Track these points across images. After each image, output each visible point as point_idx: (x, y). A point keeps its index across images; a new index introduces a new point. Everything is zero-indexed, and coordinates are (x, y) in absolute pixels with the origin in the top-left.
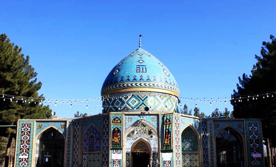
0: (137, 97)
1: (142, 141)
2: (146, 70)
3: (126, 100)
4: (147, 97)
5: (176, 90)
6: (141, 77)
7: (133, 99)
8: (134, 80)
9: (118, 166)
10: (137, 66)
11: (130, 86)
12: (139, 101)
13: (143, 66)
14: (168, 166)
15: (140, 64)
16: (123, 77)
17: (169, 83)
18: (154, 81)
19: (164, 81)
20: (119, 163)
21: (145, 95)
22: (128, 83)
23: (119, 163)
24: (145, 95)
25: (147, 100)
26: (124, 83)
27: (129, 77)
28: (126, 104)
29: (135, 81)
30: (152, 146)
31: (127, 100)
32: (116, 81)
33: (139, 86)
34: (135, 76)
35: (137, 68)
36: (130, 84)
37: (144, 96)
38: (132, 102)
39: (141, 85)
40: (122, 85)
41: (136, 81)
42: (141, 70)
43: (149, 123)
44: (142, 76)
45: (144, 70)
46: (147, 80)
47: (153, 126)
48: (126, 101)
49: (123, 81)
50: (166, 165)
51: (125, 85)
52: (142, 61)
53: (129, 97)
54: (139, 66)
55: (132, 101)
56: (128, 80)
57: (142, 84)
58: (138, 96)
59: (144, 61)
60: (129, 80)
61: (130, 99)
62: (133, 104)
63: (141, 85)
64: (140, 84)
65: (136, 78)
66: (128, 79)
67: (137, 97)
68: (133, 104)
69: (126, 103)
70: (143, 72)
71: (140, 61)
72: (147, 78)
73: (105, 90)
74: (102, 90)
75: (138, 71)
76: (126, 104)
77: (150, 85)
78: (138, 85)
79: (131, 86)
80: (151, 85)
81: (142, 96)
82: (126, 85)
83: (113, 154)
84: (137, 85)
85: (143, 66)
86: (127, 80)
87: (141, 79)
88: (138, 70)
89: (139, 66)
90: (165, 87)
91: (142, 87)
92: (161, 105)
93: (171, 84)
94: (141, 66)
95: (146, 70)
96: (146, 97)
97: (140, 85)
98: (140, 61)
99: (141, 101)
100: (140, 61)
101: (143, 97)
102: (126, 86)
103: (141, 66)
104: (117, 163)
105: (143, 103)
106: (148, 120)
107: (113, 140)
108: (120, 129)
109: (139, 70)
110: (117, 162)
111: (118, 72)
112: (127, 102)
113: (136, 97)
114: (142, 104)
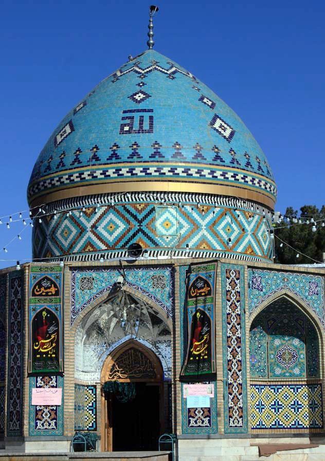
0: (121, 209)
1: (136, 347)
2: (151, 124)
3: (89, 221)
4: (153, 210)
5: (256, 182)
6: (135, 147)
7: (111, 216)
8: (110, 158)
9: (50, 424)
10: (125, 112)
11: (101, 179)
12: (128, 222)
13: (144, 111)
14: (47, 427)
15: (134, 106)
16: (79, 150)
17: (228, 161)
19: (210, 155)
20: (53, 416)
21: (147, 205)
22: (94, 167)
23: (53, 416)
24: (147, 205)
25: (153, 220)
26: (52, 175)
27: (97, 149)
28: (89, 234)
29: (114, 160)
30: (167, 363)
31: (93, 221)
32: (62, 162)
33: (129, 177)
34: (115, 145)
35: (123, 119)
36: (101, 172)
37: (142, 206)
38: (108, 228)
39: (133, 174)
40: (77, 175)
42: (136, 126)
43: (144, 291)
44: (136, 144)
45: (146, 126)
46: (153, 156)
48: (89, 225)
49: (80, 162)
50: (196, 422)
53: (99, 213)
54: (131, 111)
55: (108, 223)
56: (96, 158)
57: (137, 171)
58: (125, 209)
60: (97, 159)
61: (100, 218)
62: (111, 234)
63: (133, 174)
64: (131, 171)
65: (118, 153)
66: (95, 155)
67: (121, 209)
68: (111, 234)
69: (89, 229)
70: (141, 130)
71: (137, 97)
72: (153, 151)
73: (39, 190)
74: (29, 189)
75: (127, 128)
76: (89, 234)
77: (162, 171)
79: (103, 176)
80: (165, 170)
81: (137, 209)
82: (89, 175)
83: (34, 390)
84: (121, 172)
85: (144, 111)
86: (93, 158)
87: (132, 156)
88: (125, 125)
89: (131, 111)
90: (211, 176)
91: (135, 179)
92: (201, 233)
93: (235, 165)
94: (139, 111)
95: (151, 124)
96: (149, 208)
97: (129, 174)
98: (135, 94)
101: (140, 212)
102: (88, 178)
103: (139, 111)
104: (46, 418)
105: (140, 230)
106: (142, 284)
107: (36, 346)
108: (57, 314)
109: (128, 125)
110: (46, 415)
112: (94, 226)
113: (118, 212)
114: (137, 232)
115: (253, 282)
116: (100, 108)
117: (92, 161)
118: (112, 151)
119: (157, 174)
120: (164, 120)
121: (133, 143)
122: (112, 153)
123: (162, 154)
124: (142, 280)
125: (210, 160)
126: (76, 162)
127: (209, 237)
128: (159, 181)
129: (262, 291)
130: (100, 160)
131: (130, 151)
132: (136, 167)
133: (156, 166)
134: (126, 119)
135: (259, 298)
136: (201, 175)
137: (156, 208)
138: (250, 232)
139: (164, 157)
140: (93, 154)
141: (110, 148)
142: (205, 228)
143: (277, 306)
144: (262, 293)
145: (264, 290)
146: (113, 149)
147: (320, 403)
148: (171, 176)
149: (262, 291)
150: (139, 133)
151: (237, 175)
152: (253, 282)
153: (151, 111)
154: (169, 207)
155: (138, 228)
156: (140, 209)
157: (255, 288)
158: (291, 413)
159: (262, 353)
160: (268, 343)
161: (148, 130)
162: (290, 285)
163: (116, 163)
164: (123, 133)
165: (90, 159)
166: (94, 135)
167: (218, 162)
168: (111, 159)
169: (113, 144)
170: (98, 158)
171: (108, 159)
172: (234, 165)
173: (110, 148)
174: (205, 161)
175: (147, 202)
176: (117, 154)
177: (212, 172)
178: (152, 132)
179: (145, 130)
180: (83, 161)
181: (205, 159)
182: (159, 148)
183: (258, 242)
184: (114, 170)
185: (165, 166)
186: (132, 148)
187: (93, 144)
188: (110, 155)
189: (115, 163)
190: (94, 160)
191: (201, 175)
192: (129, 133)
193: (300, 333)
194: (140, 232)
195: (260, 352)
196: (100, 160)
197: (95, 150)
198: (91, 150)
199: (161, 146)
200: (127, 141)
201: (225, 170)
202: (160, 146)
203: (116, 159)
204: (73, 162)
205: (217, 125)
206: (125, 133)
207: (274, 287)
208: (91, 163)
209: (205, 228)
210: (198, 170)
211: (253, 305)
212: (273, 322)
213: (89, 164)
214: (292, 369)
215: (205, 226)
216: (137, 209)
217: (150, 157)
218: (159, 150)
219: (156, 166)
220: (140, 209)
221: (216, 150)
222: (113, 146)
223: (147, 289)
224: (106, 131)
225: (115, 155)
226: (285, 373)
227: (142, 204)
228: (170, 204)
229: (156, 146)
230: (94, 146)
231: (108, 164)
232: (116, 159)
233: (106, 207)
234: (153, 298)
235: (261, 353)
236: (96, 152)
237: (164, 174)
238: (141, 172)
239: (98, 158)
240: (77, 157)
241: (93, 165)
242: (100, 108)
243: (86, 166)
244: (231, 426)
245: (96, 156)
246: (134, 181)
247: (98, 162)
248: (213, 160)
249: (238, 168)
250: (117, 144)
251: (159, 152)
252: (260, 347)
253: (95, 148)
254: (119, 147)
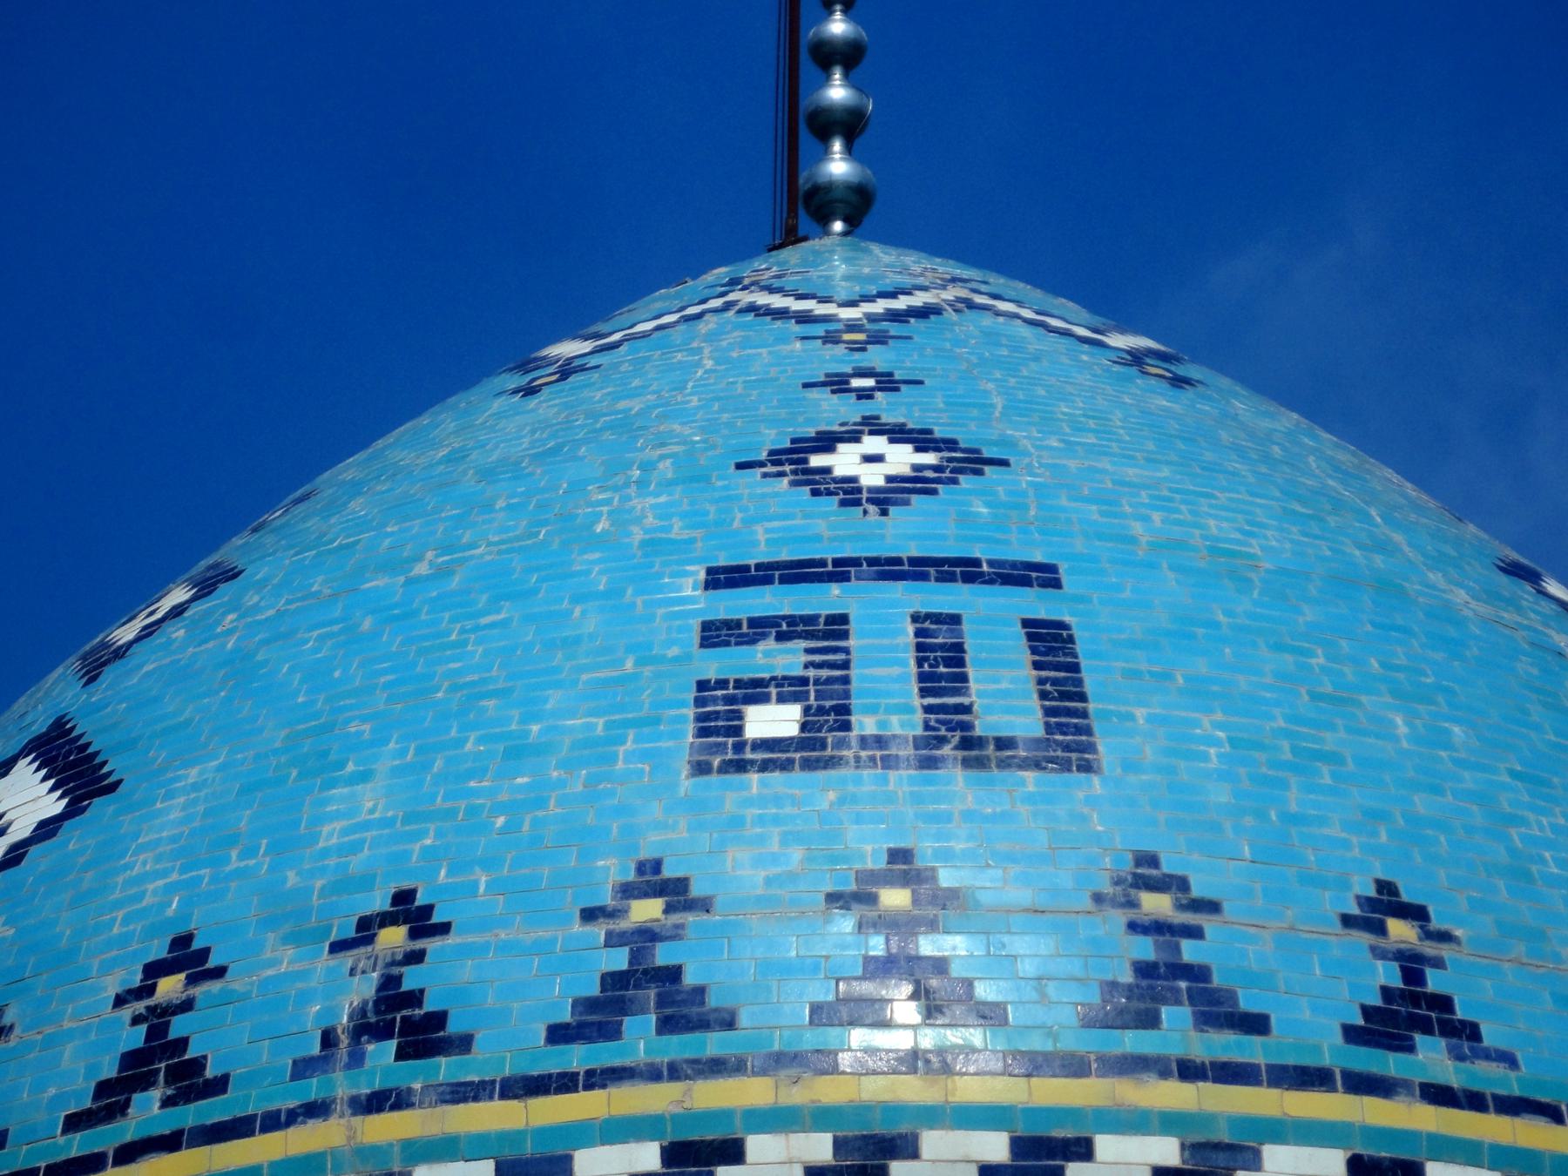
10: (722, 578)
13: (965, 570)
18: (1389, 1064)
35: (715, 634)
41: (679, 1046)
52: (922, 440)
54: (799, 572)
59: (975, 462)
71: (844, 461)
85: (965, 570)
86: (368, 1028)
88: (755, 691)
89: (799, 572)
94: (889, 569)
98: (827, 442)
100: (844, 461)
103: (889, 569)
109: (791, 688)
111: (47, 829)
116: (422, 569)
117: (357, 1059)
118: (613, 940)
120: (1201, 666)
121: (872, 855)
122: (619, 960)
123: (1231, 996)
126: (146, 1082)
130: (464, 1044)
133: (1167, 1123)
134: (752, 640)
139: (1256, 1024)
140: (365, 988)
141: (589, 915)
146: (623, 925)
150: (929, 763)
153: (1045, 576)
161: (1036, 743)
163: (675, 1072)
164: (740, 766)
165: (328, 1040)
166: (370, 800)
168: (610, 1032)
170: (439, 1019)
171: (558, 1034)
173: (589, 915)
176: (673, 974)
178: (1086, 767)
179: (1003, 743)
180: (237, 1072)
182: (1195, 933)
186: (858, 910)
187: (366, 882)
188: (594, 990)
189: (653, 1074)
190: (382, 1053)
192: (808, 765)
196: (464, 1044)
197: (393, 938)
198: (338, 947)
199: (1212, 907)
200: (785, 840)
202: (1199, 906)
203: (667, 1025)
204: (103, 1089)
206: (765, 766)
208: (342, 1084)
213: (313, 1089)
218: (1190, 951)
219: (1167, 1123)
222: (628, 891)
224: (518, 752)
229: (1157, 904)
230: (379, 902)
231: (566, 1083)
232: (667, 1025)
236: (416, 957)
239: (439, 1019)
240: (157, 1031)
241: (376, 1103)
242: (422, 569)
243: (274, 1122)
245: (415, 998)
247: (445, 1068)
250: (668, 872)
251: (1197, 974)
253: (386, 919)
254: (704, 905)
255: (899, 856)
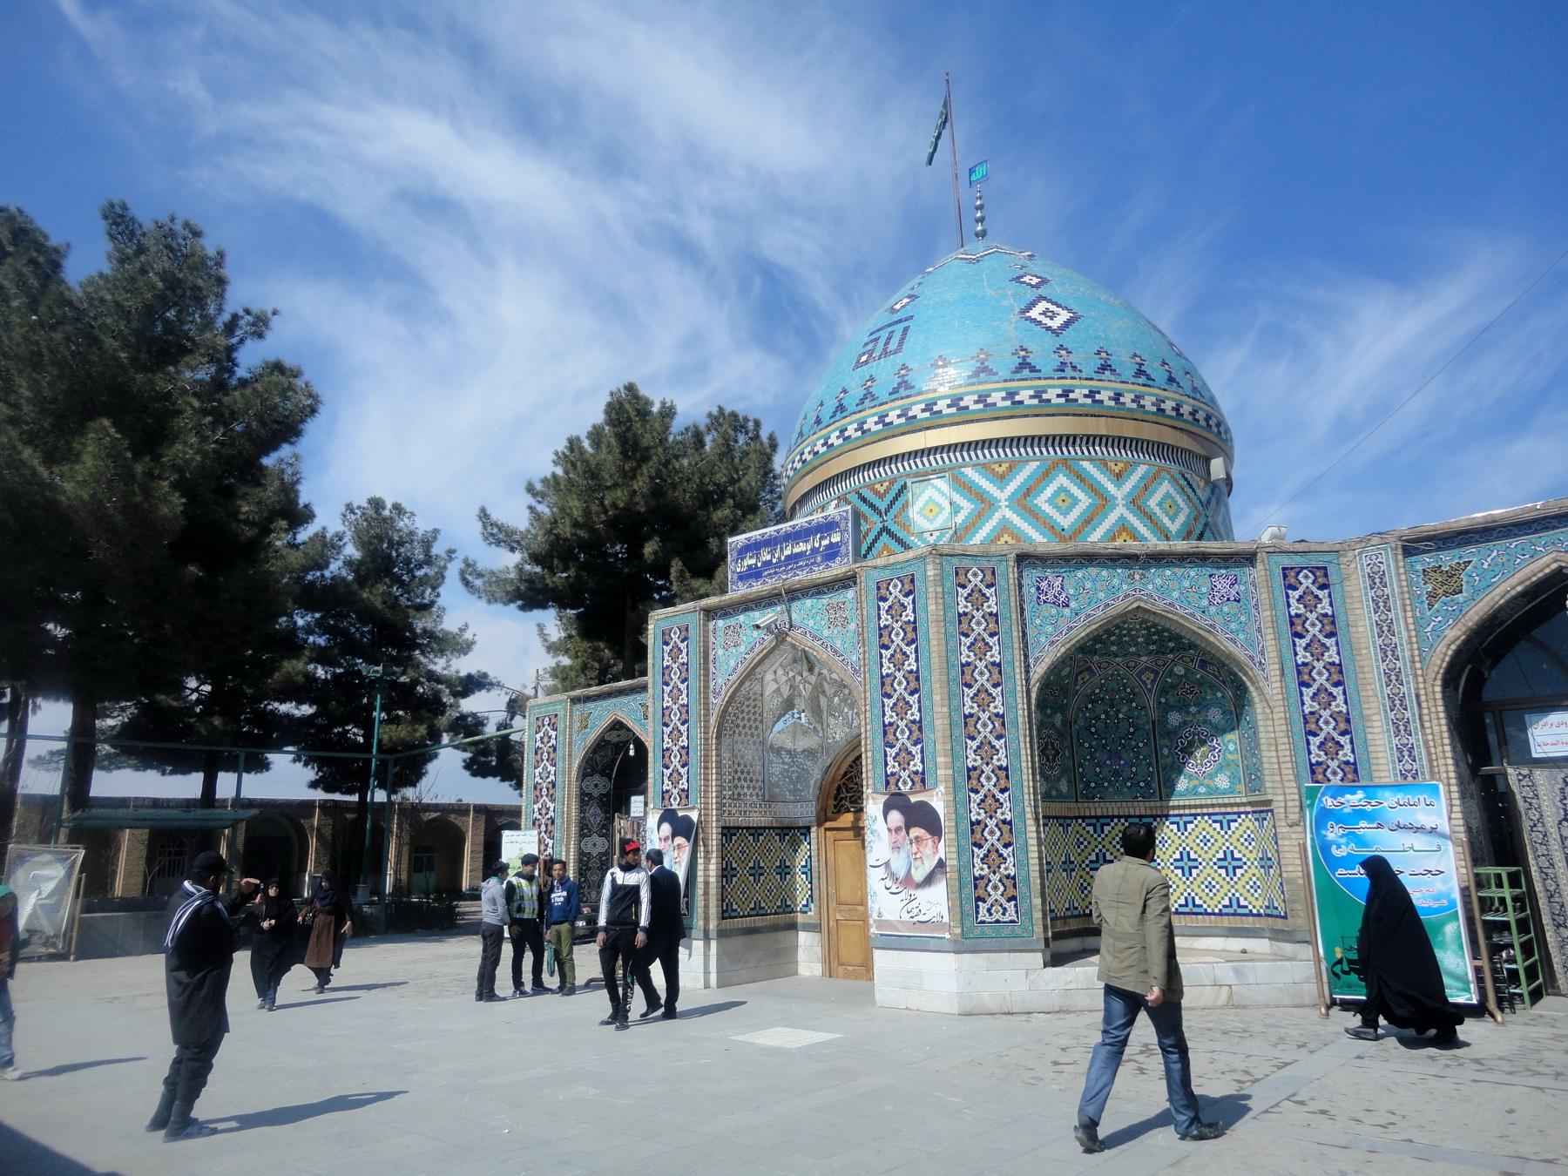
4: (904, 487)
5: (1127, 399)
21: (893, 481)
24: (893, 481)
25: (905, 506)
43: (815, 637)
44: (872, 379)
47: (836, 652)
51: (806, 451)
57: (871, 424)
78: (849, 437)
80: (916, 410)
81: (876, 492)
92: (998, 516)
96: (896, 487)
99: (876, 518)
101: (881, 496)
105: (885, 530)
106: (811, 623)
115: (1038, 588)
119: (903, 420)
124: (811, 615)
125: (1004, 373)
127: (1017, 520)
128: (908, 432)
129: (1067, 606)
131: (862, 392)
132: (868, 417)
135: (1059, 622)
136: (986, 405)
137: (909, 484)
138: (1123, 499)
142: (1007, 503)
143: (1140, 640)
144: (1066, 611)
145: (1073, 604)
147: (1276, 855)
148: (926, 419)
149: (1067, 606)
151: (1073, 392)
152: (1038, 588)
154: (931, 477)
155: (881, 526)
156: (882, 491)
157: (1045, 602)
158: (1220, 879)
159: (1141, 745)
160: (1154, 722)
162: (1150, 587)
167: (1026, 373)
169: (840, 390)
172: (1063, 375)
174: (996, 378)
175: (892, 476)
177: (1011, 395)
181: (996, 374)
183: (1150, 518)
184: (837, 433)
185: (914, 404)
191: (986, 405)
193: (1219, 695)
194: (884, 534)
195: (1133, 743)
201: (1041, 386)
205: (1034, 313)
207: (1101, 595)
209: (1007, 503)
210: (980, 396)
211: (1043, 639)
212: (1152, 676)
214: (1212, 776)
215: (1006, 500)
216: (876, 492)
217: (890, 394)
218: (906, 378)
220: (882, 491)
221: (1023, 353)
223: (819, 632)
225: (841, 408)
226: (1195, 787)
227: (885, 481)
228: (934, 472)
233: (836, 502)
234: (829, 649)
235: (1137, 746)
237: (915, 417)
238: (876, 423)
244: (983, 922)
246: (868, 444)
248: (1013, 372)
249: (1072, 378)
252: (1132, 734)
255: (941, 356)
